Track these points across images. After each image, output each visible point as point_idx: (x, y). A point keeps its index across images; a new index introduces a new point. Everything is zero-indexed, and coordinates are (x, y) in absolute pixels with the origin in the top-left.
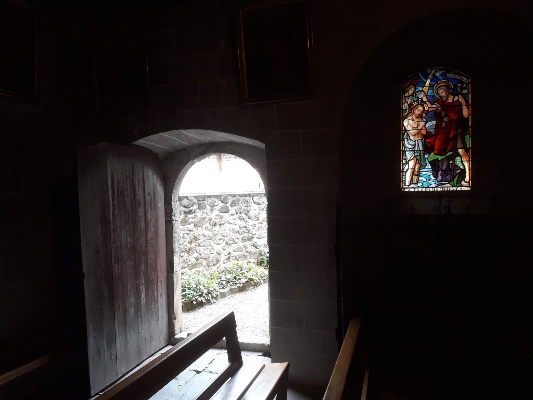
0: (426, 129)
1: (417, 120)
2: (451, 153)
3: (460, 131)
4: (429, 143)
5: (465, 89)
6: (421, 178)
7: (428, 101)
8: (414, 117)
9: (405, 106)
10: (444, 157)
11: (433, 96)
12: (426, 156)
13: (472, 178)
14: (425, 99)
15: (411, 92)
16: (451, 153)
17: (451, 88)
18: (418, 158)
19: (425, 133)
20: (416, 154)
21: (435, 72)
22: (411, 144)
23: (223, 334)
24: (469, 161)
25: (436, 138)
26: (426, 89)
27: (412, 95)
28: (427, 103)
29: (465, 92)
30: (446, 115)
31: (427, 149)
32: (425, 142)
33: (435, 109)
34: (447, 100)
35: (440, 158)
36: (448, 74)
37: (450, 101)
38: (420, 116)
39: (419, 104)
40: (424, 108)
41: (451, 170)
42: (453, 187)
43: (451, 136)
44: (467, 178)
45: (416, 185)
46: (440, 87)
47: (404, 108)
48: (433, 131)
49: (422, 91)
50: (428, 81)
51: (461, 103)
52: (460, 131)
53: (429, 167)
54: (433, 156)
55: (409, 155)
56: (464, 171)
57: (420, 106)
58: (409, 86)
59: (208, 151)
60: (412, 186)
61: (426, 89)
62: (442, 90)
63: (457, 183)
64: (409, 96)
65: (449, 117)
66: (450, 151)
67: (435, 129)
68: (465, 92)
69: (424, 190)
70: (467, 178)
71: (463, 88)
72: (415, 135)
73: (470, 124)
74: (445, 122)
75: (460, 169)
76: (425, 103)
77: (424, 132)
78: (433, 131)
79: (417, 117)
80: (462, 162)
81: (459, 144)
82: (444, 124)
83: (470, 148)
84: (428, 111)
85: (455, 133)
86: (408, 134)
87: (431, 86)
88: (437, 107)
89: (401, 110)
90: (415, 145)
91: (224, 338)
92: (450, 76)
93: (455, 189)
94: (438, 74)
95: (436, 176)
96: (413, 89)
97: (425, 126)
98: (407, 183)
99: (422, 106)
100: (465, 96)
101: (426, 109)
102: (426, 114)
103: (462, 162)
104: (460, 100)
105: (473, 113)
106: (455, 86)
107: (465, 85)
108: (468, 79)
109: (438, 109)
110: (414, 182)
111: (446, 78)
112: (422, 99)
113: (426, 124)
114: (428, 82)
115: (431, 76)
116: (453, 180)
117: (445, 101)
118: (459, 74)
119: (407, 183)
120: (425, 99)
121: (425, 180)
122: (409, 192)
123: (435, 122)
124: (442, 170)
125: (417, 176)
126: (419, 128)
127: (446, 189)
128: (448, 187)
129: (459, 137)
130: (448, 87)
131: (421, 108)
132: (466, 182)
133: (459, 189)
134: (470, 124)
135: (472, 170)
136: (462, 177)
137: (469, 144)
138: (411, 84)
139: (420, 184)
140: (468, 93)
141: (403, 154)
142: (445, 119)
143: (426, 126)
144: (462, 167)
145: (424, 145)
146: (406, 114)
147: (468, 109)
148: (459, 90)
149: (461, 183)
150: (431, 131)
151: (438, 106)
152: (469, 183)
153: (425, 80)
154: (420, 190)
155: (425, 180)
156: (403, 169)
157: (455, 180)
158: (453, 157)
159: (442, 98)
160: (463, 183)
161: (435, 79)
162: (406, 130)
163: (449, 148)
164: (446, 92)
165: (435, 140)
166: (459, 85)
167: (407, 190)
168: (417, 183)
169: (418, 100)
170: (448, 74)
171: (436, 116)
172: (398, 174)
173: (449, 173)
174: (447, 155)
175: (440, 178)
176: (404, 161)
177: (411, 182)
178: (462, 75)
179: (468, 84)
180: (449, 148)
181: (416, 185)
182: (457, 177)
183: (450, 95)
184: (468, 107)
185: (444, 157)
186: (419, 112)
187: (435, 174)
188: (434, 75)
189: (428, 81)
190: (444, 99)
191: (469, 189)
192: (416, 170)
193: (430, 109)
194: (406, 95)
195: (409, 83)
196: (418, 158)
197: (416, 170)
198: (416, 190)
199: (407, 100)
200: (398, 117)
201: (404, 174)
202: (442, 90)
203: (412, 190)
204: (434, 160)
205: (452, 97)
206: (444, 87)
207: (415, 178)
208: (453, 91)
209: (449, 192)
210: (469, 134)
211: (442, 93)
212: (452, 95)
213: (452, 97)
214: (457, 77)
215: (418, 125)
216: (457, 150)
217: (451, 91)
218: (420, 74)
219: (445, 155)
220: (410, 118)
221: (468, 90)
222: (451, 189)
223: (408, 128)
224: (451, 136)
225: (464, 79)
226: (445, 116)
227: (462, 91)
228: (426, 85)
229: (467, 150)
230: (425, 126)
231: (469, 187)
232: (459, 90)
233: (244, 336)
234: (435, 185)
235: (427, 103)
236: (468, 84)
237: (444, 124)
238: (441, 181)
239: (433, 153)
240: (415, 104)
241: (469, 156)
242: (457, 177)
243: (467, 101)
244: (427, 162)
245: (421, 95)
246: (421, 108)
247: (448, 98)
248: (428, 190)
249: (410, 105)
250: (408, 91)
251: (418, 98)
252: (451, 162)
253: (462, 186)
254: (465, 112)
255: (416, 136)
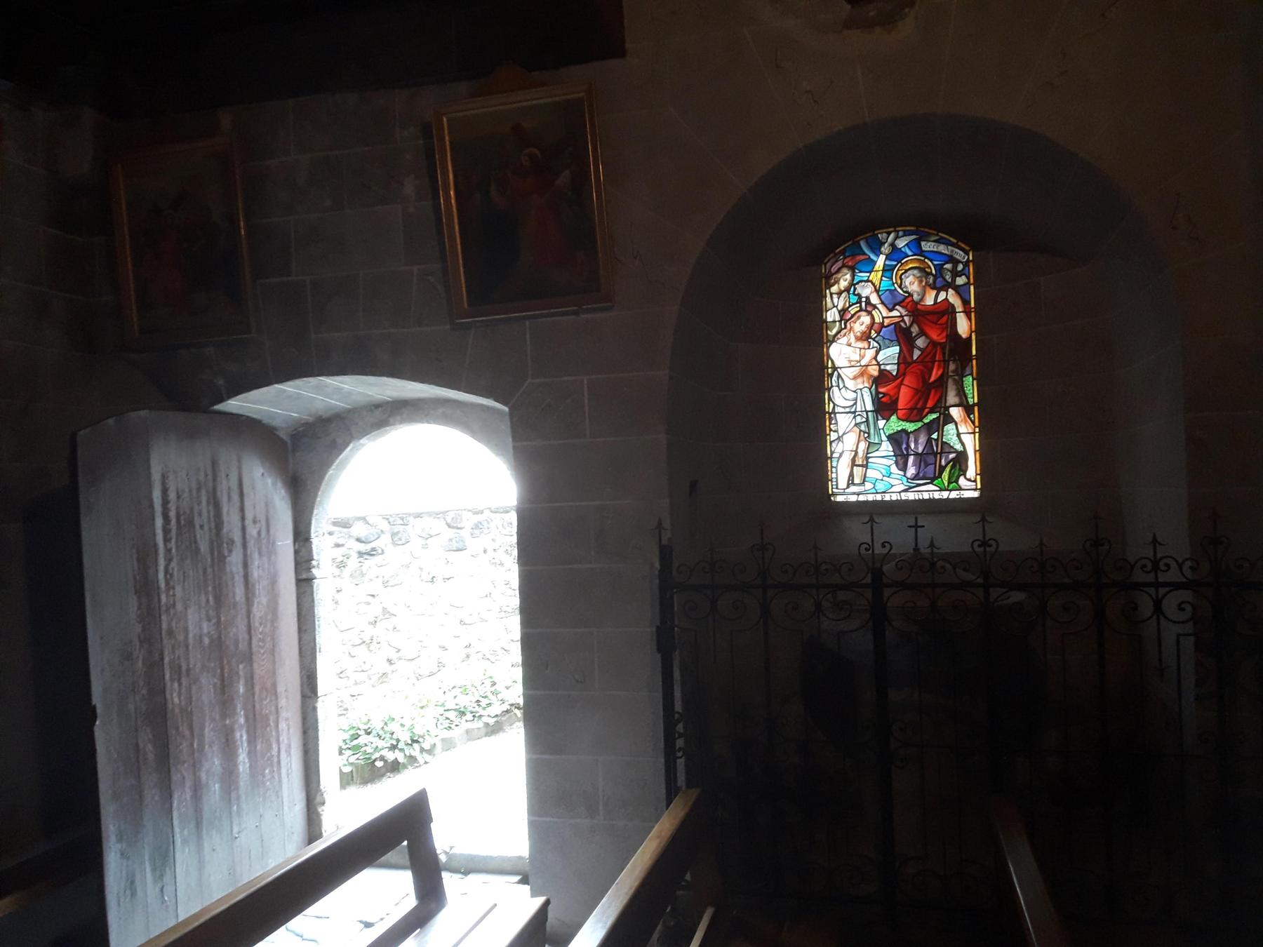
0: (879, 364)
1: (860, 344)
2: (934, 416)
3: (952, 367)
4: (885, 394)
5: (960, 274)
6: (870, 473)
7: (882, 303)
8: (853, 339)
9: (832, 315)
10: (920, 424)
11: (893, 292)
12: (881, 423)
13: (984, 471)
14: (874, 299)
15: (843, 284)
16: (934, 416)
17: (931, 273)
18: (863, 427)
19: (876, 373)
20: (859, 419)
21: (897, 238)
22: (848, 395)
23: (402, 835)
24: (974, 433)
25: (901, 383)
26: (876, 277)
27: (847, 290)
28: (880, 306)
29: (961, 281)
30: (922, 333)
31: (884, 407)
32: (877, 393)
33: (897, 320)
34: (922, 300)
35: (911, 427)
36: (923, 243)
37: (929, 301)
38: (865, 337)
39: (861, 310)
40: (873, 318)
41: (935, 454)
42: (941, 490)
43: (933, 379)
44: (972, 471)
45: (861, 489)
46: (906, 271)
47: (829, 319)
48: (892, 368)
49: (868, 281)
50: (882, 257)
51: (953, 306)
52: (952, 367)
53: (886, 448)
54: (895, 424)
55: (844, 422)
56: (961, 458)
57: (863, 313)
58: (838, 271)
59: (339, 441)
60: (853, 489)
61: (876, 277)
62: (911, 278)
63: (949, 483)
64: (840, 294)
65: (927, 336)
66: (932, 411)
67: (898, 364)
68: (961, 281)
69: (879, 497)
70: (972, 471)
71: (956, 274)
72: (855, 378)
73: (974, 352)
74: (920, 349)
75: (956, 451)
76: (875, 307)
77: (874, 371)
78: (892, 368)
79: (858, 339)
80: (959, 435)
81: (952, 398)
82: (917, 354)
83: (974, 405)
84: (882, 325)
85: (940, 372)
86: (839, 376)
87: (887, 270)
88: (901, 316)
89: (823, 324)
90: (856, 399)
91: (405, 843)
92: (927, 246)
93: (945, 495)
94: (901, 243)
95: (904, 468)
96: (848, 277)
97: (875, 358)
98: (843, 483)
99: (870, 313)
100: (957, 289)
101: (877, 320)
102: (878, 333)
103: (959, 435)
104: (951, 300)
105: (980, 329)
106: (940, 268)
107: (960, 267)
108: (967, 253)
109: (903, 321)
110: (857, 481)
111: (921, 253)
112: (867, 298)
113: (877, 353)
114: (881, 261)
115: (886, 249)
116: (940, 476)
117: (917, 303)
118: (948, 243)
119: (843, 483)
120: (874, 299)
121: (880, 477)
122: (846, 504)
123: (897, 349)
124: (916, 454)
125: (863, 464)
126: (863, 363)
127: (926, 496)
128: (929, 492)
129: (950, 382)
130: (924, 271)
131: (866, 319)
132: (969, 480)
133: (954, 495)
134: (974, 352)
135: (983, 452)
136: (960, 469)
137: (973, 395)
138: (844, 266)
139: (868, 486)
140: (968, 284)
141: (830, 419)
142: (921, 342)
143: (879, 358)
144: (958, 447)
145: (876, 400)
146: (834, 331)
147: (970, 319)
148: (948, 277)
149: (957, 481)
150: (888, 368)
151: (904, 313)
152: (975, 481)
153: (873, 257)
154: (870, 498)
155: (880, 477)
156: (832, 453)
157: (946, 475)
158: (937, 426)
159: (910, 295)
160: (962, 481)
161: (895, 254)
162: (835, 368)
163: (930, 404)
164: (921, 282)
165: (898, 388)
166: (948, 266)
167: (840, 499)
168: (863, 483)
169: (859, 302)
170: (923, 243)
171: (902, 336)
172: (818, 461)
173: (931, 459)
174: (926, 421)
175: (911, 471)
176: (834, 436)
177: (851, 481)
178: (953, 245)
179: (966, 264)
180: (930, 404)
181: (861, 489)
182: (948, 469)
183: (928, 289)
184: (967, 313)
185: (920, 424)
186: (863, 328)
187: (901, 462)
188: (893, 245)
189: (882, 257)
190: (916, 297)
191: (976, 494)
192: (861, 454)
193: (887, 322)
194: (834, 289)
195: (839, 264)
196: (863, 427)
197: (861, 454)
198: (862, 498)
199: (835, 300)
200: (814, 338)
201: (834, 464)
202: (911, 278)
203: (853, 498)
204: (898, 432)
205: (934, 293)
206: (915, 272)
207: (858, 472)
208: (934, 282)
209: (931, 501)
210: (971, 374)
211: (912, 284)
212: (933, 288)
213: (934, 293)
214: (942, 248)
215: (862, 357)
216: (947, 408)
217: (931, 280)
218: (863, 244)
219: (921, 420)
220: (844, 340)
221: (968, 278)
222: (937, 495)
223: (838, 364)
224: (933, 379)
225: (959, 255)
226: (919, 336)
227: (954, 280)
228: (876, 268)
229: (968, 410)
230: (875, 358)
231: (976, 489)
232: (948, 277)
233: (445, 837)
234: (902, 487)
235: (880, 306)
236: (966, 264)
237: (917, 354)
238: (916, 477)
239: (894, 418)
240: (853, 310)
241: (973, 423)
242: (948, 469)
243: (966, 302)
244: (884, 438)
245: (866, 291)
246: (866, 319)
247: (924, 295)
248: (887, 498)
249: (843, 312)
250: (837, 282)
251: (859, 296)
252: (935, 436)
253: (960, 489)
254: (963, 326)
255: (860, 380)
